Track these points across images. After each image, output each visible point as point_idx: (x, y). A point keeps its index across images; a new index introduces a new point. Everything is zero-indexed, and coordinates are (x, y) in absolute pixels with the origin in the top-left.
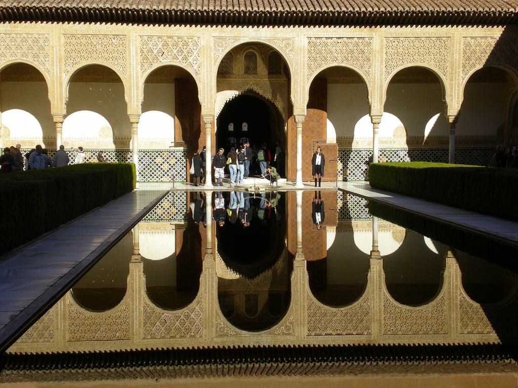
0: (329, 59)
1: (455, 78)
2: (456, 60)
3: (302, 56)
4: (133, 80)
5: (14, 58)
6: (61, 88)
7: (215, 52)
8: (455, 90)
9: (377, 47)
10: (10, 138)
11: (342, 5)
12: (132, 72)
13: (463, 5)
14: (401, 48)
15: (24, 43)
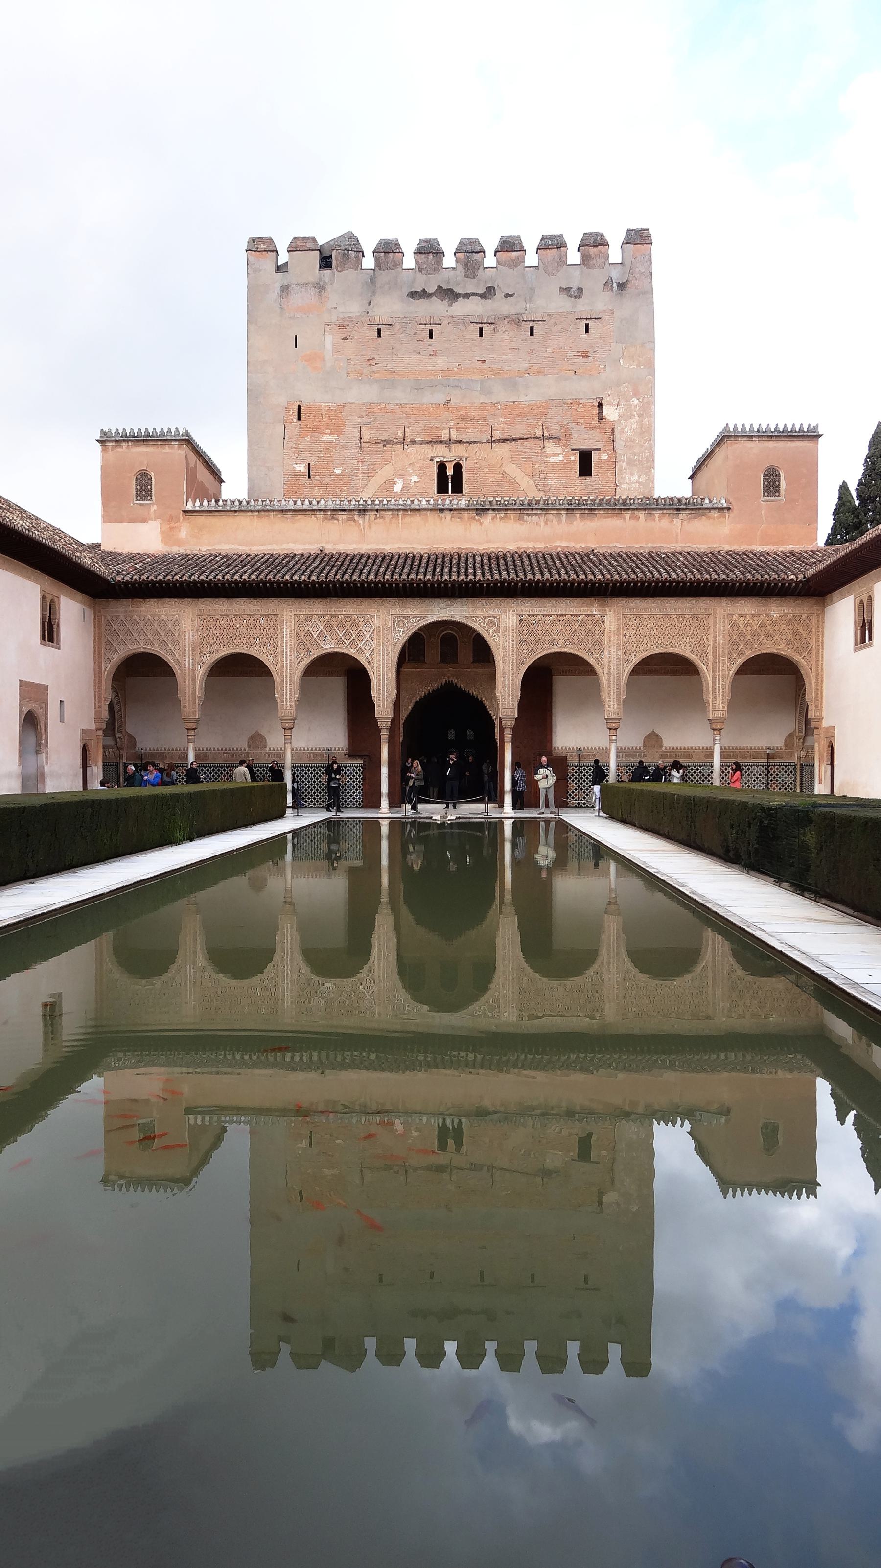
0: (547, 642)
1: (719, 669)
2: (719, 644)
3: (511, 639)
4: (287, 672)
5: (136, 647)
6: (194, 684)
7: (394, 634)
8: (719, 684)
9: (612, 627)
10: (137, 749)
11: (563, 571)
12: (285, 662)
13: (727, 571)
14: (645, 628)
15: (149, 628)
